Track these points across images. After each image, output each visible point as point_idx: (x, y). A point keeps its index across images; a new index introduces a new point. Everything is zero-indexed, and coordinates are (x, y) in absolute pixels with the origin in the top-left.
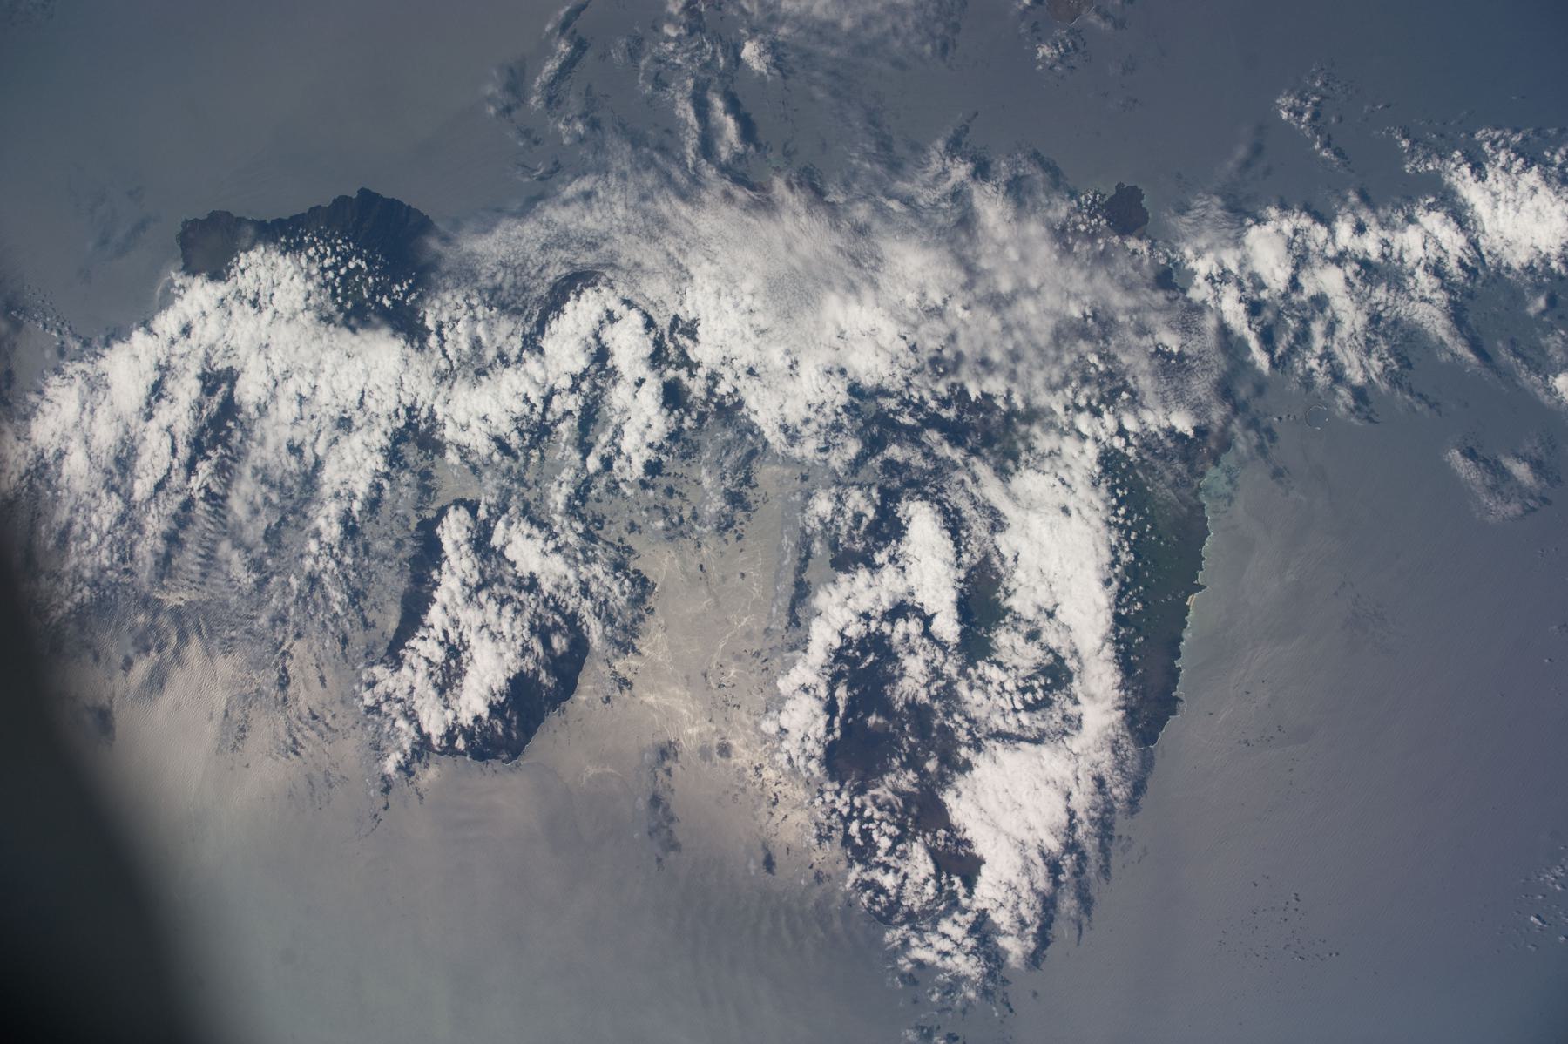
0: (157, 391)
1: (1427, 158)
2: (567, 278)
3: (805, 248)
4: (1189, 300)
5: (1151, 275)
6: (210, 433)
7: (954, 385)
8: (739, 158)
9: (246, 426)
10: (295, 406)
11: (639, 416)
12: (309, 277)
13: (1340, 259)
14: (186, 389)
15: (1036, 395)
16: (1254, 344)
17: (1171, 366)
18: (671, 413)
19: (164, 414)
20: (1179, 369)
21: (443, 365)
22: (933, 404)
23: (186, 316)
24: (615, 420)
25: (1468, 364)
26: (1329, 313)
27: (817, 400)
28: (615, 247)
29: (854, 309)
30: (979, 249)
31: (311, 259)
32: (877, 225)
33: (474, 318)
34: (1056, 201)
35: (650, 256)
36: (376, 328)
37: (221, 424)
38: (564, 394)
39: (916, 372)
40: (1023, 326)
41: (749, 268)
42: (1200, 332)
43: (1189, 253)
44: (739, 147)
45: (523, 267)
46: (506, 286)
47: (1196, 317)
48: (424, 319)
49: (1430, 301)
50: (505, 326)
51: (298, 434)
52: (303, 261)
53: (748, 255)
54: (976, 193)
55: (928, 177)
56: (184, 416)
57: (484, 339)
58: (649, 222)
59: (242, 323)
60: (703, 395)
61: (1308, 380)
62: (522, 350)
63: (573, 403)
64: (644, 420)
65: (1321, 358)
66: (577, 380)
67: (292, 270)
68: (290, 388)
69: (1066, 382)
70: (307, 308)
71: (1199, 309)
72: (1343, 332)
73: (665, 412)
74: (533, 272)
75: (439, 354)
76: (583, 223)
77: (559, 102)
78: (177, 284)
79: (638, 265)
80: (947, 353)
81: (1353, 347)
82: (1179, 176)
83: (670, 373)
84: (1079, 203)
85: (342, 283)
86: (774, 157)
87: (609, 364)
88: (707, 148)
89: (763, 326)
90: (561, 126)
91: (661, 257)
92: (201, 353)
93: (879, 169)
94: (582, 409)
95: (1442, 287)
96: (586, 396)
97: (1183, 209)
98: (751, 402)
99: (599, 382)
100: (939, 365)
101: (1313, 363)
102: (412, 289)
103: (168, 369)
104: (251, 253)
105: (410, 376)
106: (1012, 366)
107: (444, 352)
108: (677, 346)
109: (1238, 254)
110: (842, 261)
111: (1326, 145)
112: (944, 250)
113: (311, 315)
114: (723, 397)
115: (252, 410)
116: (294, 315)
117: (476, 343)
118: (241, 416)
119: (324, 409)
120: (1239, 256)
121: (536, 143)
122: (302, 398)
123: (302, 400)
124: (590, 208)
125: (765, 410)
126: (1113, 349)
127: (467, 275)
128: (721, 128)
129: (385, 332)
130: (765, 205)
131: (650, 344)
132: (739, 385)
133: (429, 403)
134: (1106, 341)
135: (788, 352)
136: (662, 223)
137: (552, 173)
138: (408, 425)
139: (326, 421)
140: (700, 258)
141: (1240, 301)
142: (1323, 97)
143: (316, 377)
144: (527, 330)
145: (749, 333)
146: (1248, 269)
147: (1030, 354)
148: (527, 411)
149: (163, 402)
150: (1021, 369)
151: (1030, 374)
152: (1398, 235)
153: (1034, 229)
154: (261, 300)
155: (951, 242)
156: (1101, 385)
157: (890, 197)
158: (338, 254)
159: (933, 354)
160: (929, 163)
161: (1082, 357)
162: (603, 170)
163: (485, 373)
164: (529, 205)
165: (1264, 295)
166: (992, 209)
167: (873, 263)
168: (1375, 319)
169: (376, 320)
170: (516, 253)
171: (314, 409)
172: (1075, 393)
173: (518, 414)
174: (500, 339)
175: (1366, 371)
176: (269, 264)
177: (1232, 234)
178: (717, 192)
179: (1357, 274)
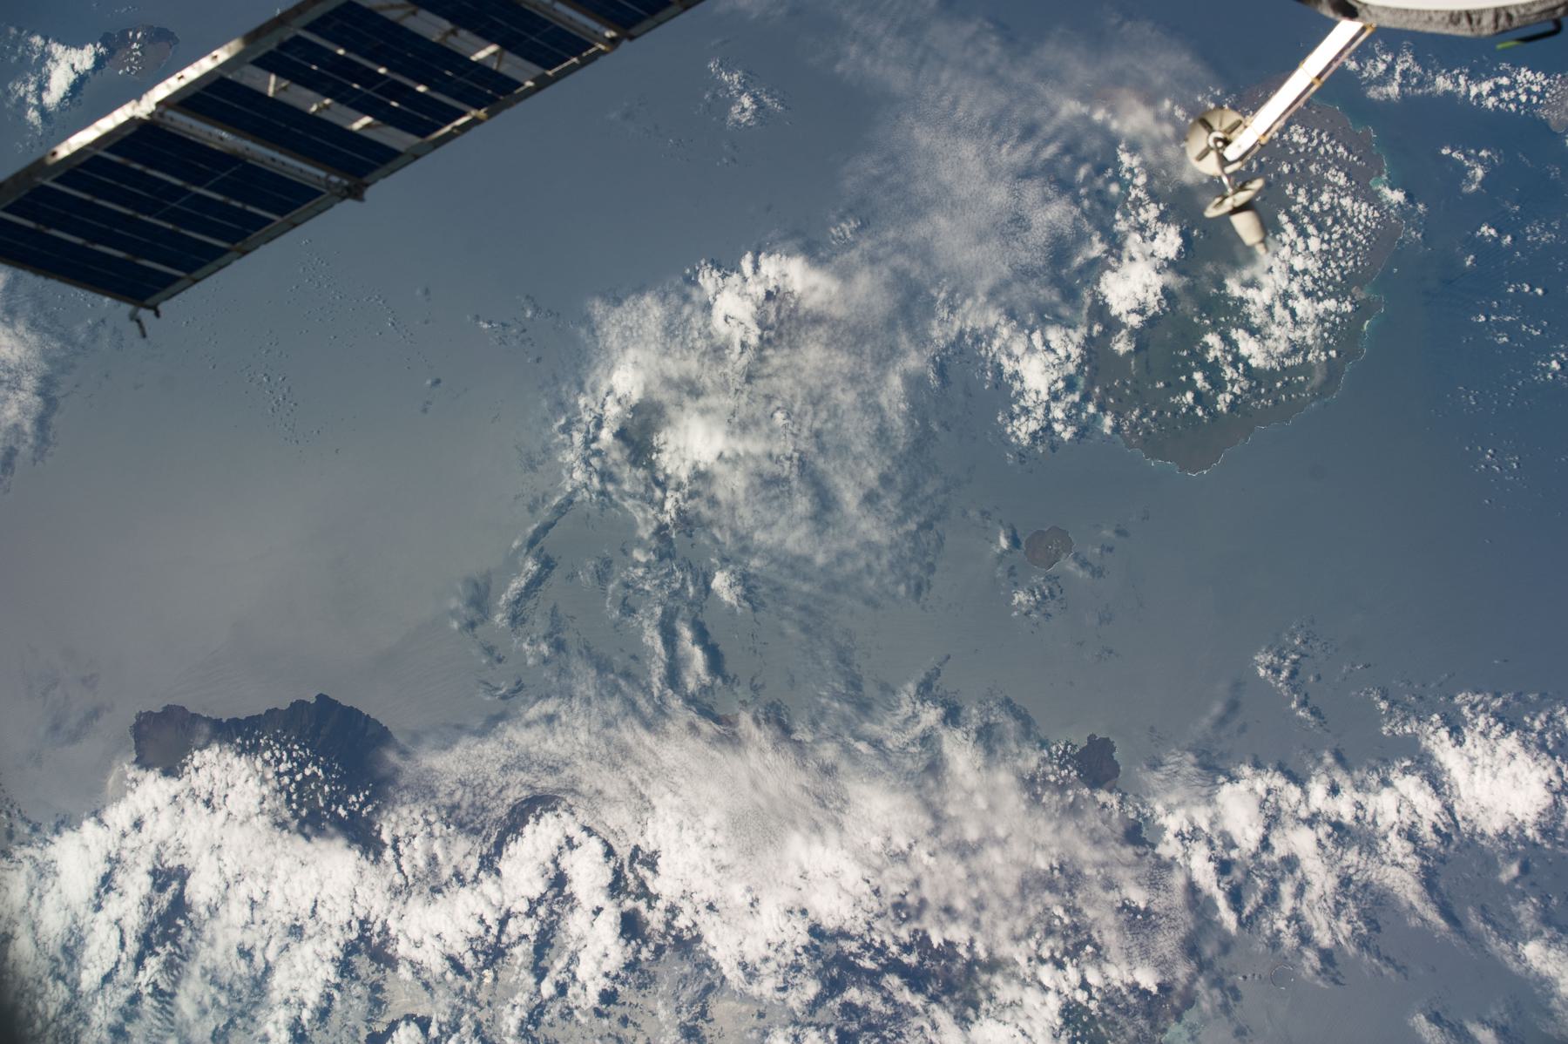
0: (106, 882)
1: (1405, 720)
2: (527, 800)
3: (771, 784)
4: (1158, 857)
5: (1120, 830)
6: (159, 929)
7: (916, 931)
8: (705, 689)
9: (196, 924)
10: (247, 910)
11: (595, 945)
12: (264, 781)
13: (1312, 821)
14: (136, 883)
15: (999, 945)
16: (1222, 903)
17: (1138, 921)
18: (628, 942)
19: (113, 906)
20: (1146, 926)
21: (399, 880)
22: (894, 949)
23: (137, 810)
24: (571, 947)
25: (1437, 929)
26: (1298, 874)
27: (776, 939)
28: (577, 772)
29: (817, 849)
30: (947, 796)
31: (267, 763)
32: (844, 766)
33: (431, 835)
34: (1027, 750)
35: (612, 784)
36: (331, 837)
37: (170, 923)
38: (520, 917)
39: (878, 916)
40: (988, 875)
41: (712, 802)
42: (1167, 889)
43: (1159, 808)
44: (707, 679)
45: (482, 786)
46: (464, 805)
47: (1165, 874)
48: (379, 832)
49: (1402, 866)
50: (462, 845)
51: (249, 939)
52: (259, 763)
53: (712, 789)
54: (945, 739)
55: (897, 720)
56: (134, 910)
57: (441, 857)
58: (612, 749)
59: (195, 822)
60: (662, 928)
61: (1275, 942)
62: (479, 870)
63: (529, 927)
64: (601, 949)
65: (1289, 919)
66: (533, 905)
67: (247, 772)
68: (242, 891)
69: (1030, 933)
70: (261, 812)
71: (1168, 866)
72: (1312, 894)
73: (622, 942)
74: (493, 793)
75: (394, 868)
76: (545, 747)
77: (524, 621)
78: (130, 776)
79: (599, 792)
80: (910, 899)
81: (1322, 909)
82: (1152, 729)
83: (629, 904)
84: (1050, 754)
85: (297, 790)
86: (742, 691)
87: (567, 890)
88: (673, 677)
89: (725, 862)
90: (525, 646)
91: (623, 786)
92: (152, 849)
93: (848, 709)
94: (538, 934)
95: (1415, 852)
96: (542, 921)
97: (1155, 765)
98: (710, 937)
99: (556, 908)
100: (902, 910)
101: (1281, 924)
102: (368, 800)
103: (118, 861)
104: (206, 752)
105: (364, 889)
106: (976, 914)
107: (399, 867)
108: (636, 877)
109: (1209, 812)
110: (808, 801)
111: (1303, 704)
112: (911, 795)
113: (265, 819)
114: (681, 930)
115: (202, 910)
116: (248, 818)
117: (433, 860)
118: (191, 916)
119: (276, 915)
120: (1210, 814)
121: (500, 660)
122: (253, 902)
123: (253, 904)
124: (553, 732)
125: (724, 946)
126: (1079, 903)
127: (425, 790)
128: (690, 658)
129: (340, 842)
130: (730, 739)
131: (609, 873)
132: (697, 919)
133: (382, 917)
134: (1072, 894)
135: (749, 890)
136: (625, 751)
137: (514, 692)
138: (361, 938)
139: (278, 927)
140: (663, 789)
141: (1210, 859)
142: (1303, 655)
143: (268, 882)
144: (485, 851)
145: (710, 868)
146: (1219, 827)
147: (995, 904)
148: (482, 932)
149: (113, 895)
150: (985, 918)
151: (994, 924)
152: (1372, 798)
153: (1004, 778)
154: (215, 801)
155: (919, 787)
156: (1065, 937)
157: (858, 738)
158: (294, 760)
159: (897, 899)
160: (899, 707)
161: (1047, 909)
162: (567, 694)
163: (440, 891)
164: (491, 724)
165: (1234, 854)
166: (961, 755)
167: (838, 804)
168: (1345, 881)
169: (331, 830)
170: (476, 773)
171: (266, 914)
172: (1039, 945)
173: (473, 935)
174: (457, 858)
175: (1334, 934)
176: (223, 765)
177: (1205, 791)
178: (682, 724)
179: (1329, 836)
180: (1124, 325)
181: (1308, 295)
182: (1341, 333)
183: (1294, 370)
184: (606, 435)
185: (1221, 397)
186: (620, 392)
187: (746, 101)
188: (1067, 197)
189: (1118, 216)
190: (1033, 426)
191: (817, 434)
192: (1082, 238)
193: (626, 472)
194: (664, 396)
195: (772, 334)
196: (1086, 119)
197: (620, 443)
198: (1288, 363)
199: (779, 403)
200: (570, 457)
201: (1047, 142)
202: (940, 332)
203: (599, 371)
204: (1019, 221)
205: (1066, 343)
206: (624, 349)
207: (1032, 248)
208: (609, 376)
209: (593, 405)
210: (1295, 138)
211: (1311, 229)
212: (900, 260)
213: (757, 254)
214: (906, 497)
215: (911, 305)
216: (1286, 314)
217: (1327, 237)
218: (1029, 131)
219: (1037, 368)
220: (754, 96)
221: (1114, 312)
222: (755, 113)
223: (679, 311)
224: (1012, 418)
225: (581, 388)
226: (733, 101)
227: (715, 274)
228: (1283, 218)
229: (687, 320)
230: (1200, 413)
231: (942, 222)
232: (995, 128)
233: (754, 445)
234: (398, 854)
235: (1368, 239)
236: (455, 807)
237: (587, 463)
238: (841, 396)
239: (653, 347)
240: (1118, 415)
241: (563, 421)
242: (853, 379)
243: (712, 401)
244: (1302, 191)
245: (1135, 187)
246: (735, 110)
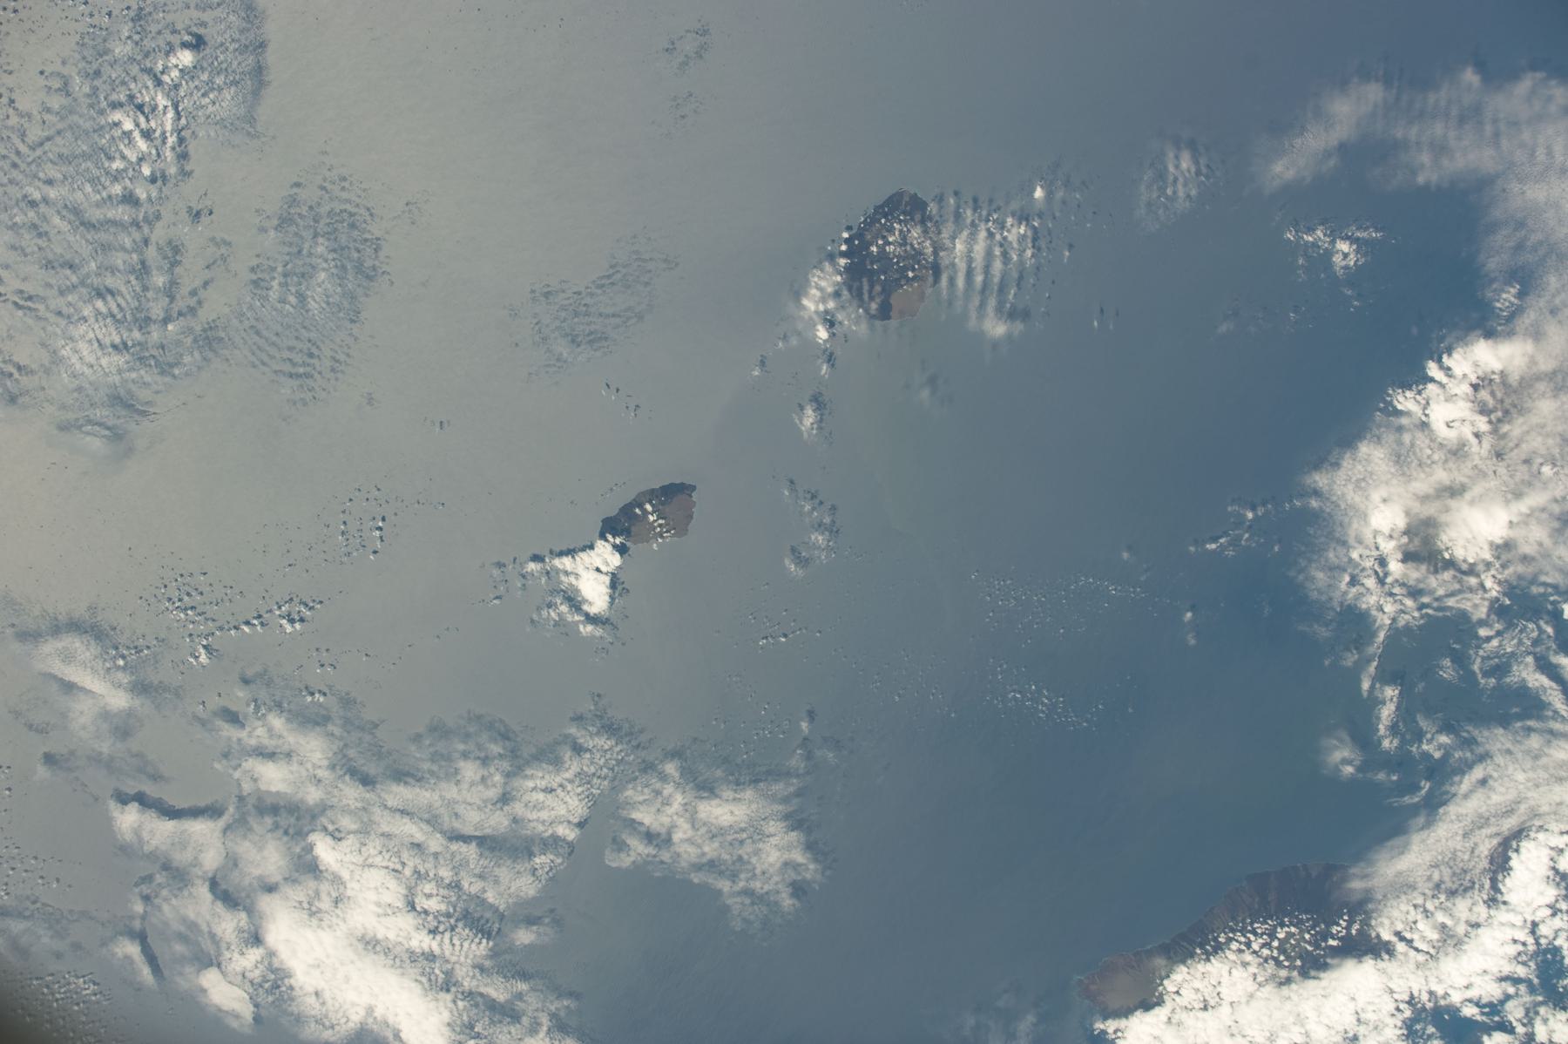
46: (1446, 879)
48: (1378, 936)
50: (1462, 906)
57: (1449, 922)
74: (1466, 857)
102: (1350, 923)
107: (1417, 950)
117: (1444, 926)
127: (1404, 887)
170: (1442, 853)
184: (1395, 567)
186: (1387, 531)
187: (1344, 246)
193: (1433, 582)
194: (1430, 510)
197: (1410, 565)
200: (1372, 600)
203: (1355, 526)
206: (1367, 498)
209: (1367, 552)
213: (1439, 361)
220: (1347, 238)
222: (1357, 251)
223: (1400, 443)
225: (1344, 543)
226: (1329, 254)
227: (1408, 394)
229: (1412, 445)
234: (1409, 942)
236: (1438, 886)
237: (1391, 594)
239: (1394, 482)
241: (1347, 579)
246: (1337, 259)
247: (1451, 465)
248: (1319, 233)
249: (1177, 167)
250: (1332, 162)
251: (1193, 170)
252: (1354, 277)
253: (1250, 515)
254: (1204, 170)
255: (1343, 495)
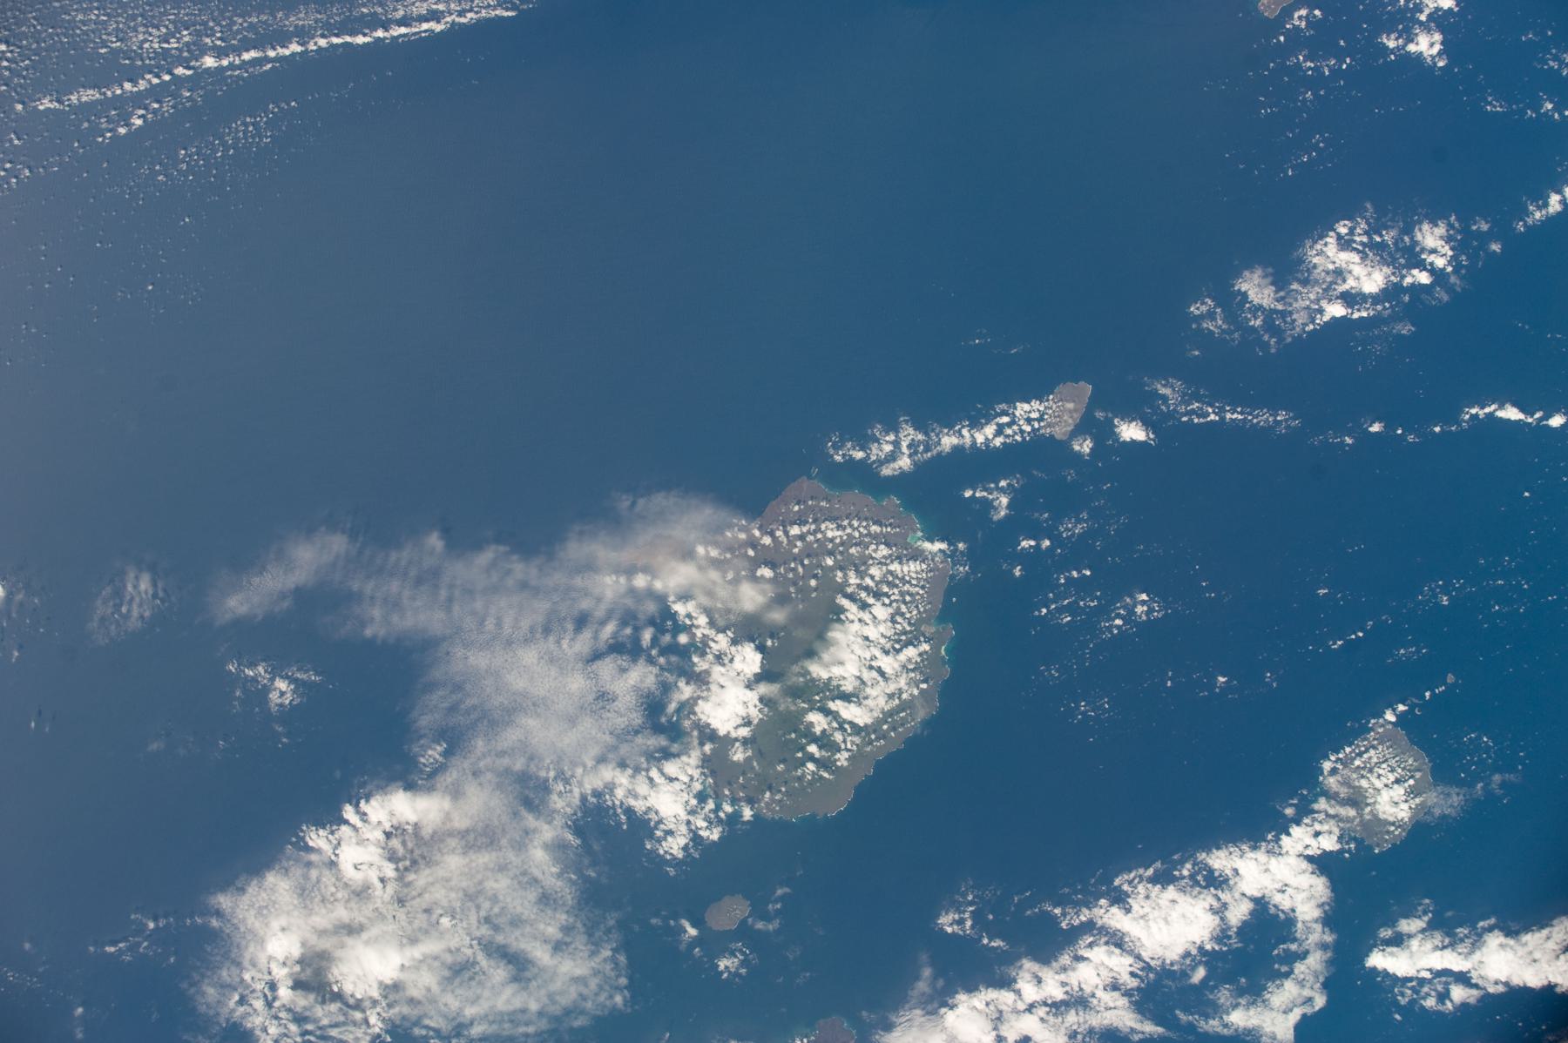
180: (736, 740)
181: (887, 653)
182: (923, 668)
183: (891, 713)
185: (838, 756)
187: (282, 685)
188: (642, 662)
189: (695, 659)
190: (682, 841)
191: (487, 920)
192: (666, 688)
194: (325, 944)
195: (408, 863)
196: (632, 591)
198: (887, 708)
199: (440, 911)
201: (603, 623)
202: (563, 802)
204: (604, 698)
205: (686, 768)
206: (267, 925)
207: (626, 711)
208: (263, 948)
210: (830, 534)
211: (871, 601)
212: (506, 761)
213: (357, 806)
214: (590, 935)
215: (529, 792)
216: (874, 674)
217: (887, 601)
218: (581, 622)
219: (670, 801)
220: (286, 677)
221: (722, 732)
222: (294, 692)
223: (306, 877)
224: (659, 841)
226: (266, 690)
227: (321, 832)
228: (845, 603)
229: (318, 881)
230: (826, 775)
231: (531, 722)
232: (547, 631)
233: (430, 947)
235: (923, 587)
238: (495, 885)
239: (296, 913)
240: (751, 801)
242: (502, 868)
243: (374, 931)
244: (852, 574)
245: (698, 627)
246: (274, 696)
247: (352, 904)
248: (261, 669)
249: (135, 587)
250: (286, 604)
251: (151, 592)
252: (288, 715)
253: (151, 925)
254: (161, 594)
255: (244, 919)
